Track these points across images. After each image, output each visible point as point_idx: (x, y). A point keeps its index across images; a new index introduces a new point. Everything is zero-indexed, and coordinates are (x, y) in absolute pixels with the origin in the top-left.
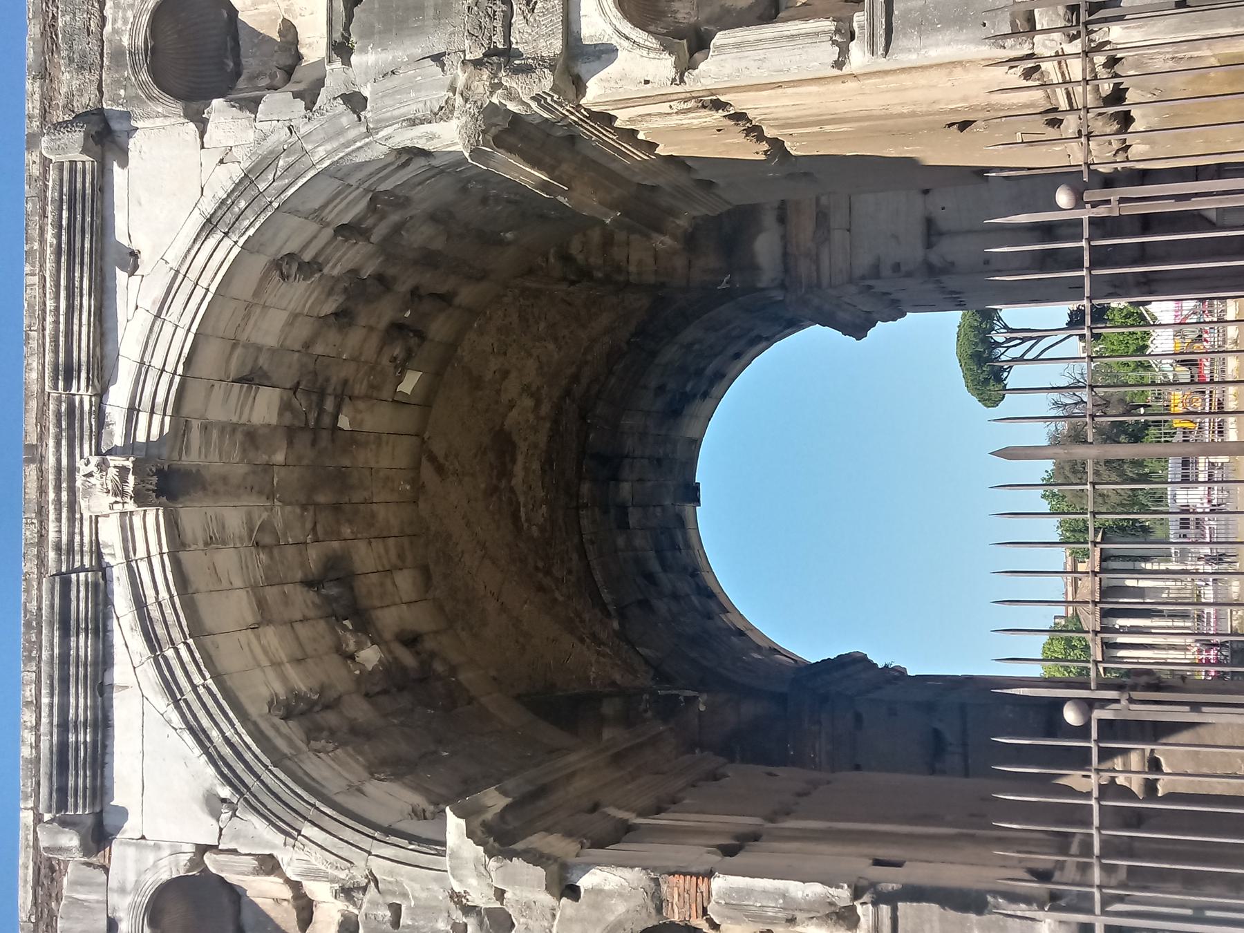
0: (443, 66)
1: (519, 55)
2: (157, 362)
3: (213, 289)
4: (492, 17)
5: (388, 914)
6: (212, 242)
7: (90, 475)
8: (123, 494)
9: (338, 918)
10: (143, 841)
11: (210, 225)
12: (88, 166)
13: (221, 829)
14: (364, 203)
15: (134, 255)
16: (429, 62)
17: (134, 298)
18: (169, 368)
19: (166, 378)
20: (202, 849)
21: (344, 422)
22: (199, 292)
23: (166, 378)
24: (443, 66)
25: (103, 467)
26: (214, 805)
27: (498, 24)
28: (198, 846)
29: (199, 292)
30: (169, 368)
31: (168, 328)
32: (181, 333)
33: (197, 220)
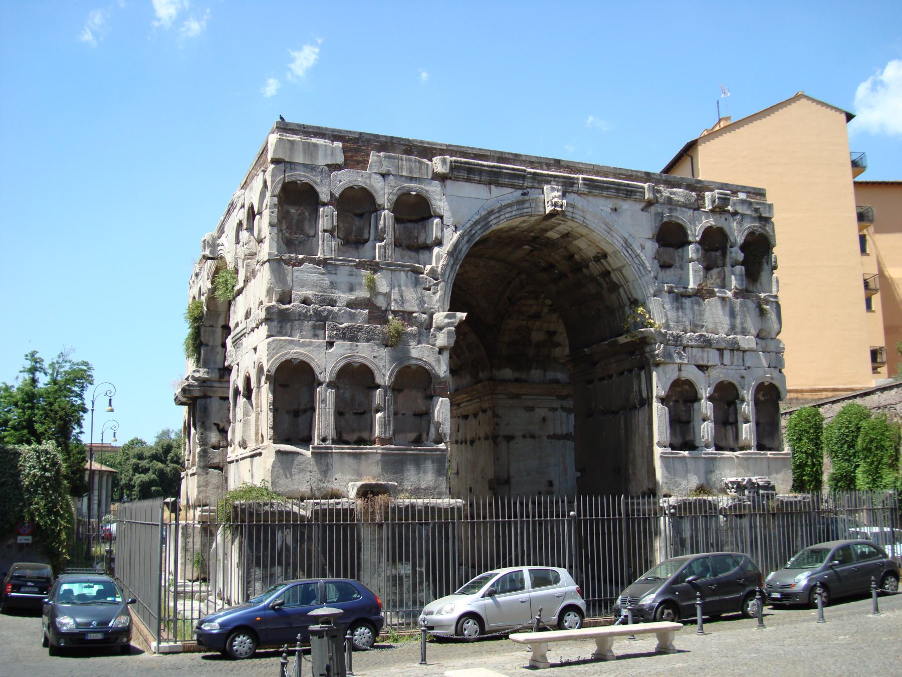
6: (620, 240)
11: (626, 241)
14: (616, 280)
20: (441, 217)
21: (526, 247)
33: (626, 236)
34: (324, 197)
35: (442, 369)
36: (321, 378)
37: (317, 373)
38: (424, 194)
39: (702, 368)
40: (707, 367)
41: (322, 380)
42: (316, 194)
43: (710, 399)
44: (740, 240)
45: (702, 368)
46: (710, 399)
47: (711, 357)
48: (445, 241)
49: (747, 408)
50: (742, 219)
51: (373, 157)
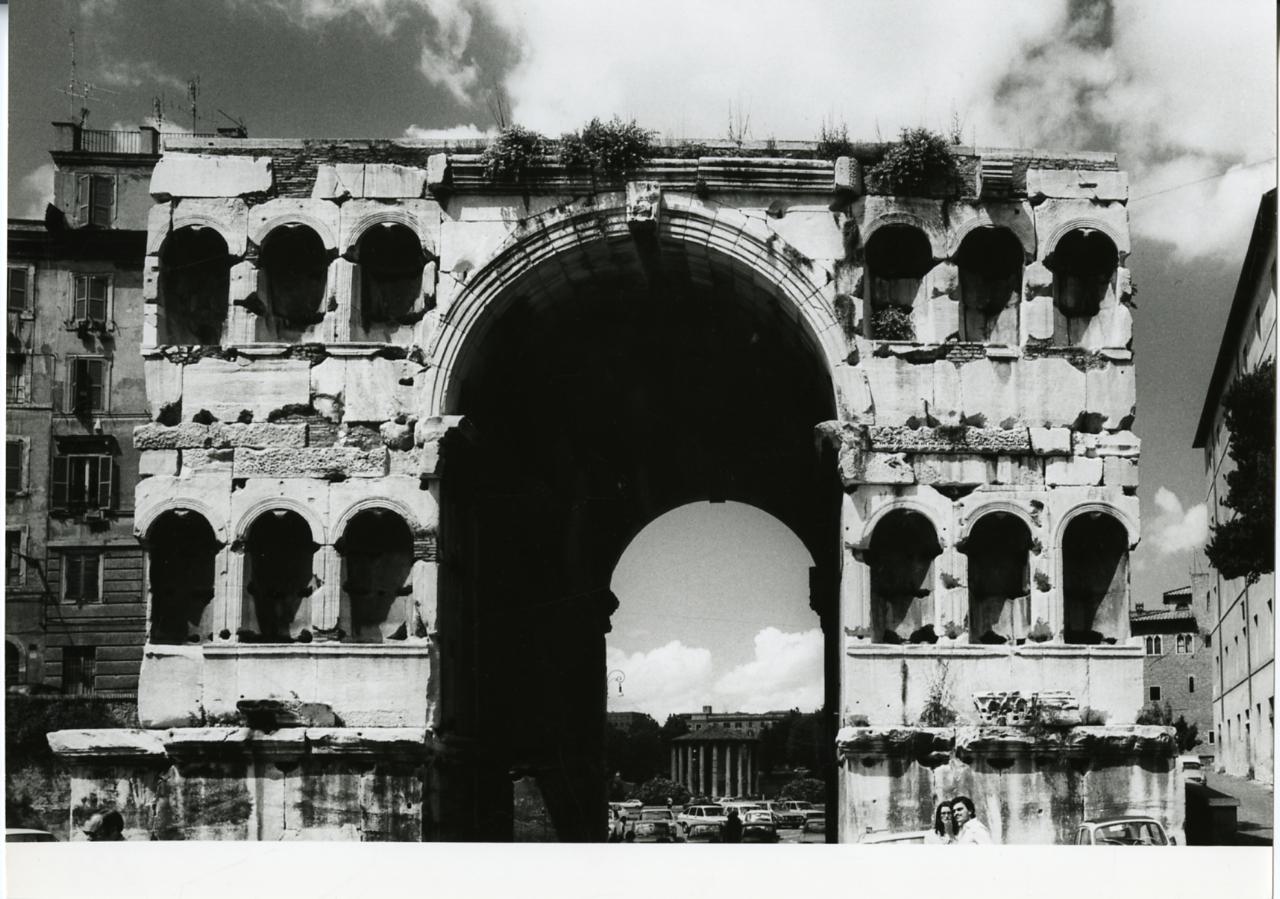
0: (867, 412)
1: (868, 460)
2: (715, 231)
3: (755, 267)
4: (889, 443)
5: (407, 377)
7: (649, 188)
8: (635, 213)
9: (404, 346)
10: (439, 221)
12: (832, 187)
13: (449, 273)
15: (780, 216)
16: (870, 404)
17: (752, 219)
18: (712, 239)
19: (705, 236)
20: (437, 260)
22: (753, 258)
23: (705, 236)
24: (867, 412)
25: (652, 199)
26: (463, 267)
27: (886, 445)
28: (439, 257)
29: (753, 258)
30: (712, 239)
31: (733, 238)
32: (731, 246)
34: (236, 247)
35: (423, 511)
36: (221, 537)
37: (216, 529)
38: (407, 222)
39: (955, 492)
40: (967, 490)
41: (223, 541)
42: (222, 244)
43: (961, 547)
44: (1045, 248)
45: (955, 492)
46: (961, 547)
47: (973, 471)
48: (439, 300)
49: (1047, 562)
50: (1053, 208)
51: (324, 172)
